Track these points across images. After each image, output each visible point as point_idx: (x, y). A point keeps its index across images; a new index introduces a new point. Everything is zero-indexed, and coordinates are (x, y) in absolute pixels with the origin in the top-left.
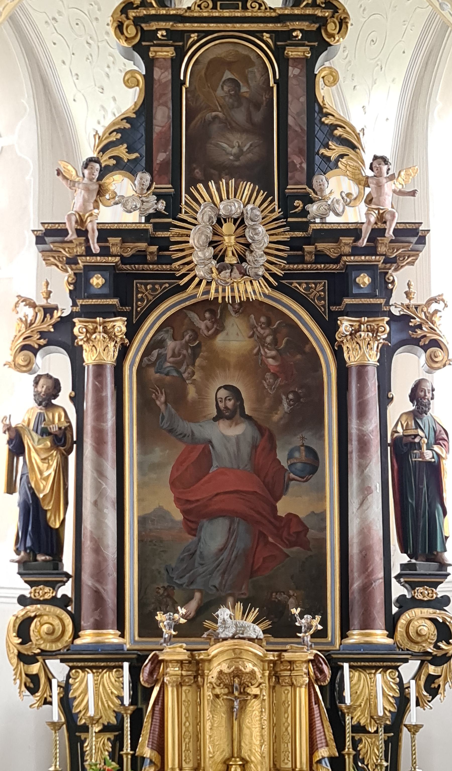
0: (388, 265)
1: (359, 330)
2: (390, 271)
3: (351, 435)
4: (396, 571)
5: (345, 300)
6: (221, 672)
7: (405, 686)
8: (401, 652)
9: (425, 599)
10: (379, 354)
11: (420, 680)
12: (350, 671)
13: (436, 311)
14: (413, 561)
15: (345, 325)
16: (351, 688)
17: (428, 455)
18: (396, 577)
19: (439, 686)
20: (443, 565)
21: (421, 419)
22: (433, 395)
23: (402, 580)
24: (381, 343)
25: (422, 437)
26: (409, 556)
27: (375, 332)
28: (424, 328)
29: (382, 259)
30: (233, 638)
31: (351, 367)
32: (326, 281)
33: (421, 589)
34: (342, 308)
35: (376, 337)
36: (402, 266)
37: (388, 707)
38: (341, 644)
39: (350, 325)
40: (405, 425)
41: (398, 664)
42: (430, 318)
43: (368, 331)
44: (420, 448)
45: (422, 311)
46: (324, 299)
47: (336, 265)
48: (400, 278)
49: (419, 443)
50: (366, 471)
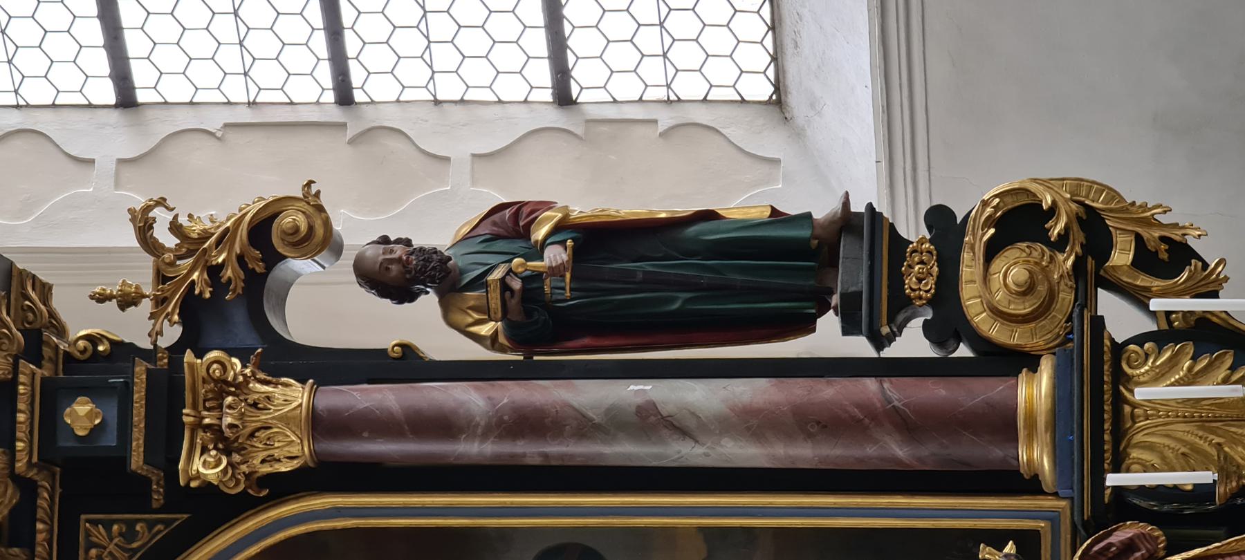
0: (47, 351)
1: (216, 430)
2: (63, 346)
3: (498, 456)
4: (860, 347)
5: (133, 467)
7: (1165, 327)
8: (1075, 337)
9: (936, 269)
10: (284, 379)
11: (1147, 289)
12: (1128, 471)
13: (175, 228)
14: (835, 299)
15: (203, 467)
16: (1173, 470)
17: (556, 255)
18: (879, 348)
19: (1163, 239)
20: (847, 222)
21: (462, 272)
22: (398, 241)
23: (885, 330)
24: (253, 374)
25: (510, 271)
26: (822, 312)
27: (222, 387)
28: (220, 260)
29: (27, 367)
31: (315, 454)
32: (83, 517)
33: (910, 281)
34: (156, 476)
35: (238, 386)
36: (52, 314)
37: (1222, 373)
38: (1055, 494)
39: (202, 454)
40: (476, 316)
41: (1107, 342)
42: (191, 244)
43: (220, 407)
44: (537, 276)
45: (172, 264)
46: (131, 524)
47: (40, 490)
48: (82, 320)
49: (525, 280)
50: (597, 420)
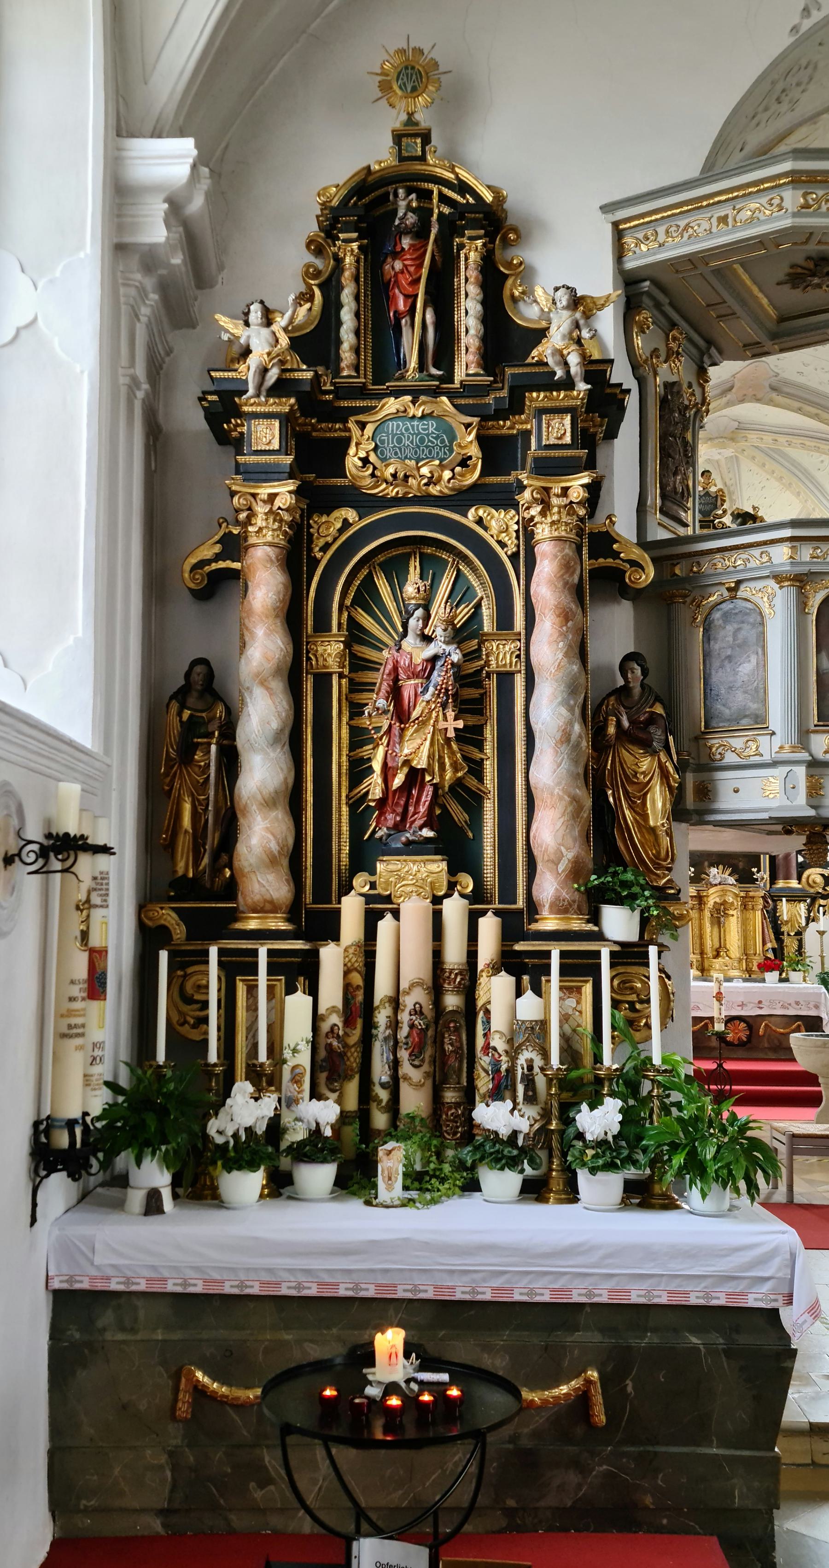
6: (715, 903)
30: (720, 884)
